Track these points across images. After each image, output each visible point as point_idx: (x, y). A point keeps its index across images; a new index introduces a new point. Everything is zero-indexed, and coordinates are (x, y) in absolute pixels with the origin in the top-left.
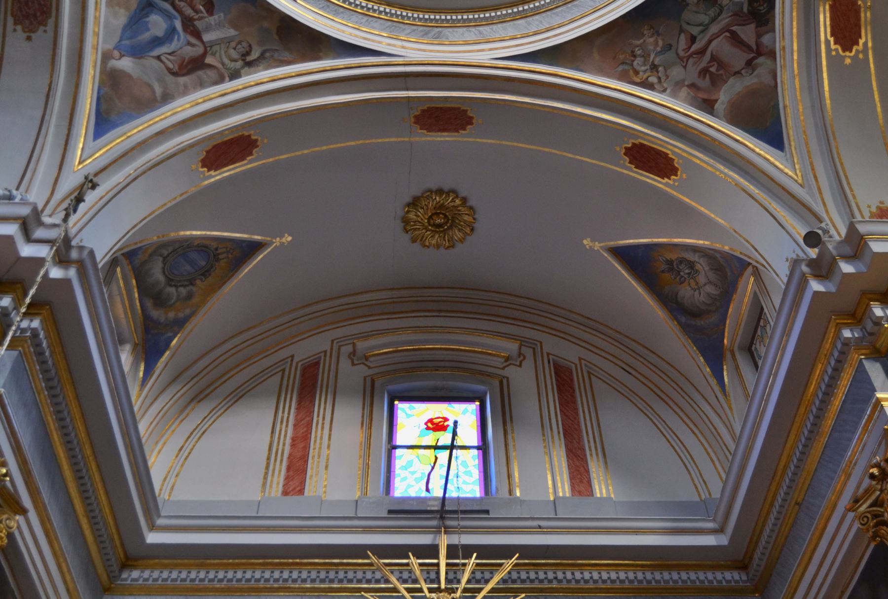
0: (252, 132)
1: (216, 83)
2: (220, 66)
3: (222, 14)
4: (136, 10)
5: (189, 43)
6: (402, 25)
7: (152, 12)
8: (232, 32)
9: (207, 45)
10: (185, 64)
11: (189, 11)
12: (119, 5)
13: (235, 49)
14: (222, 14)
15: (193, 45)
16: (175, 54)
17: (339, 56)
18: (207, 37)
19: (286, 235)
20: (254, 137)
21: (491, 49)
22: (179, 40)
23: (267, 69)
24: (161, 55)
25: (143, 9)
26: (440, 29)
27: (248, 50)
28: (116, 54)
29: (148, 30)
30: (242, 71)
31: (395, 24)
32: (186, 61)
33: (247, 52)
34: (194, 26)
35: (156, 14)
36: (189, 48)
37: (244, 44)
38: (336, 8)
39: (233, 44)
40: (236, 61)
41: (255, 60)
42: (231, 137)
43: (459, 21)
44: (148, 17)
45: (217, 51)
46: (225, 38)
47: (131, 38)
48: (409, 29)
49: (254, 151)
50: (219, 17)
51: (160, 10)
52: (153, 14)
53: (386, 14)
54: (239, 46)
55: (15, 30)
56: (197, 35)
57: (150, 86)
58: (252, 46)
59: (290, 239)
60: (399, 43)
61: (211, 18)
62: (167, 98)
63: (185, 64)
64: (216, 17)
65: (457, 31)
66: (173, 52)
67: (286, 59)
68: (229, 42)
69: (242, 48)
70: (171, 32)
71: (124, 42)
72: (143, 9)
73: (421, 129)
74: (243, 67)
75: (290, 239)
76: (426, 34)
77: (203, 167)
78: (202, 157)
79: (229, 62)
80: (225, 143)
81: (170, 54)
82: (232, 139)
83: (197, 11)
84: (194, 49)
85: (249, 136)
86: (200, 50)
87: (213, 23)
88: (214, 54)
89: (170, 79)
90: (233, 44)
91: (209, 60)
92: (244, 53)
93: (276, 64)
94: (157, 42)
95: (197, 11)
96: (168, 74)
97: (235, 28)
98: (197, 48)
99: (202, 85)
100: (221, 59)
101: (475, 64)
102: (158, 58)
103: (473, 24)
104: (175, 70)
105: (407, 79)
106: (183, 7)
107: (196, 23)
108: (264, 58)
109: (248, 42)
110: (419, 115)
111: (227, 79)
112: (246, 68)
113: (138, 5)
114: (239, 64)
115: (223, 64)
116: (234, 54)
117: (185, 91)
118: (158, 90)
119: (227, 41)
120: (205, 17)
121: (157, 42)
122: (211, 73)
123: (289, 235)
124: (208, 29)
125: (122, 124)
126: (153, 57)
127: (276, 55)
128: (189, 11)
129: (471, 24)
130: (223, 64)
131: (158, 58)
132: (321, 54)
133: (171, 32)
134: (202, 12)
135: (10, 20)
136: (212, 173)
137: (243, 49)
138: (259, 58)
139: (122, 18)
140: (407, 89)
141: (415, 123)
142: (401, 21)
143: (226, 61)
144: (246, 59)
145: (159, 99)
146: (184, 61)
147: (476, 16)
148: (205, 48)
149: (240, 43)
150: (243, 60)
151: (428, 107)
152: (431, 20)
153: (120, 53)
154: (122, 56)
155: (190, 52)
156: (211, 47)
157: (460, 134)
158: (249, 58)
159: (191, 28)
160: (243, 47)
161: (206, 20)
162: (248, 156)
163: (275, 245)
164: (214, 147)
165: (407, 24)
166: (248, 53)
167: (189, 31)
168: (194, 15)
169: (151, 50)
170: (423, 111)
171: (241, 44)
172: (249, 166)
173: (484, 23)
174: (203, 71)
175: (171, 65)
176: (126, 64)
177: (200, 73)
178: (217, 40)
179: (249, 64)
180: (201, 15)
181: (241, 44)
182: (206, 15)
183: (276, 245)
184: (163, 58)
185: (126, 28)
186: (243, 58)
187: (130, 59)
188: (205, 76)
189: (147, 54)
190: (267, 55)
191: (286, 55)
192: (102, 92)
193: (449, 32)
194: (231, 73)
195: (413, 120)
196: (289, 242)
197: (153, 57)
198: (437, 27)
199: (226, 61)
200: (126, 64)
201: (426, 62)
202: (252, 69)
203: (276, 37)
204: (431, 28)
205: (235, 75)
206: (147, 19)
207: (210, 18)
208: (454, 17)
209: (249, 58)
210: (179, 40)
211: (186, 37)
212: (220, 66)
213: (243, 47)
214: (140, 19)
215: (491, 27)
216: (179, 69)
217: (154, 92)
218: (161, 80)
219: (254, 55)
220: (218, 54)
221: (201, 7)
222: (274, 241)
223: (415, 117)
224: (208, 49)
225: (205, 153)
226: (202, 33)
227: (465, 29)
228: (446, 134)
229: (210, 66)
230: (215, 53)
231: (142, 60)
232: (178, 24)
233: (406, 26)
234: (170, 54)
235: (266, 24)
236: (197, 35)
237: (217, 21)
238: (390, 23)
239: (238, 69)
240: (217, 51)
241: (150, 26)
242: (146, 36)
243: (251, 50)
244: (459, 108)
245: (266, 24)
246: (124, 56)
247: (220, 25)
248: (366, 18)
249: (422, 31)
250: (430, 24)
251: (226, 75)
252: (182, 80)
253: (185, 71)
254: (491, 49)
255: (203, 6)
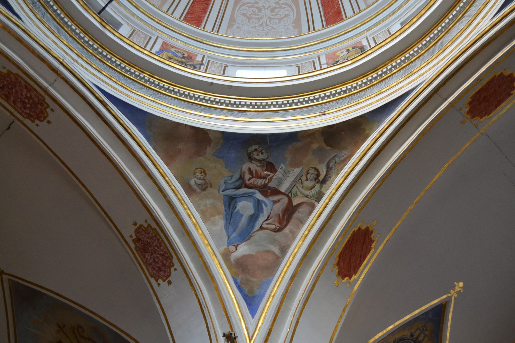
0: (359, 225)
1: (310, 213)
2: (305, 199)
3: (282, 165)
4: (225, 210)
5: (275, 202)
6: (412, 64)
7: (236, 202)
8: (298, 170)
9: (287, 194)
10: (281, 218)
11: (260, 182)
12: (212, 215)
13: (307, 180)
14: (282, 165)
15: (278, 201)
16: (271, 216)
17: (380, 122)
18: (283, 189)
19: (455, 283)
20: (364, 228)
21: (483, 18)
22: (266, 206)
23: (338, 174)
24: (262, 225)
25: (230, 205)
26: (441, 41)
27: (316, 173)
28: (232, 248)
29: (242, 215)
30: (323, 190)
31: (406, 68)
32: (281, 215)
33: (316, 175)
34: (269, 188)
35: (240, 201)
36: (277, 205)
37: (312, 171)
38: (358, 95)
39: (304, 178)
40: (313, 187)
41: (326, 176)
42: (347, 240)
43: (448, 23)
44: (236, 207)
45: (296, 192)
46: (296, 178)
47: (235, 230)
48: (418, 62)
49: (372, 237)
50: (282, 168)
51: (241, 197)
52: (238, 203)
53: (395, 67)
54: (309, 176)
55: (159, 285)
56: (276, 192)
57: (268, 251)
58: (317, 168)
59: (461, 284)
60: (416, 76)
61: (278, 173)
62: (284, 250)
63: (281, 218)
64: (279, 170)
65: (453, 32)
66: (268, 217)
67: (345, 156)
68: (300, 179)
69: (311, 176)
70: (258, 204)
71: (231, 237)
72: (230, 205)
73: (481, 118)
74: (321, 187)
75: (461, 284)
76: (433, 53)
77: (343, 278)
78: (337, 271)
79: (310, 191)
80: (346, 247)
81: (267, 220)
82: (349, 241)
83: (265, 178)
84: (280, 203)
85: (359, 229)
86: (285, 200)
87: (280, 176)
88: (296, 195)
89: (278, 236)
90: (304, 178)
91: (295, 203)
92: (315, 177)
93: (342, 166)
94: (253, 218)
95: (265, 178)
96: (276, 233)
97: (297, 165)
98: (282, 201)
99: (302, 222)
100: (303, 194)
101: (478, 37)
102: (261, 228)
103: (460, 16)
104: (278, 228)
105: (438, 92)
106: (254, 183)
107: (270, 185)
108: (331, 169)
109: (312, 167)
110: (470, 110)
111: (316, 203)
112: (324, 185)
113: (225, 206)
114: (318, 186)
115: (307, 196)
116: (309, 184)
117: (294, 235)
118: (276, 250)
119: (299, 179)
120: (273, 176)
121: (253, 218)
122: (303, 209)
123: (458, 282)
124: (280, 182)
125: (265, 291)
126: (258, 230)
127: (337, 159)
128: (260, 182)
129: (459, 17)
130: (307, 196)
131: (261, 228)
132: (367, 132)
133: (258, 204)
134: (269, 175)
135: (153, 280)
136: (354, 277)
137: (313, 175)
138: (327, 172)
139: (220, 222)
140: (446, 100)
141: (473, 117)
142: (409, 62)
143: (307, 192)
144: (319, 180)
145: (280, 255)
146: (279, 215)
147: (458, 9)
148: (287, 196)
149: (307, 173)
150: (317, 183)
151: (471, 98)
152: (429, 42)
153: (234, 245)
154: (236, 247)
155: (279, 208)
156: (291, 192)
157: (514, 95)
158: (321, 178)
159: (269, 191)
160: (312, 174)
161: (275, 177)
162: (371, 245)
163: (453, 298)
164: (340, 256)
165: (415, 60)
166: (318, 175)
167: (269, 194)
168: (265, 181)
169: (253, 227)
170: (470, 103)
171: (309, 173)
172: (378, 251)
173: (467, 8)
174: (297, 212)
175: (273, 227)
176: (243, 249)
177: (296, 215)
178: (291, 184)
179: (324, 181)
180: (268, 178)
181: (309, 173)
182: (272, 174)
183: (455, 297)
184: (264, 226)
185: (226, 227)
186: (317, 181)
187: (243, 244)
188: (301, 215)
189: (252, 232)
190: (331, 164)
191: (344, 153)
192: (239, 281)
193: (447, 37)
194: (316, 198)
195: (469, 117)
196: (463, 287)
197: (258, 230)
198: (437, 42)
199: (307, 192)
200: (243, 249)
201: (443, 69)
202: (328, 183)
203: (329, 148)
204: (433, 47)
205: (319, 196)
206: (237, 209)
207: (276, 174)
208: (443, 25)
209: (321, 178)
210: (266, 206)
211: (269, 200)
212: (305, 199)
213: (312, 174)
214: (232, 213)
215: (474, 5)
216: (280, 223)
217: (274, 253)
218: (274, 242)
219: (323, 172)
220: (298, 193)
221: (265, 172)
222: (449, 295)
223: (469, 112)
224: (290, 195)
225: (337, 267)
226: (278, 188)
227: (457, 25)
228: (503, 104)
229: (299, 205)
230: (296, 193)
231: (252, 239)
232: (259, 196)
233: (416, 62)
234: (267, 220)
235: (315, 146)
236: (276, 192)
237: (283, 172)
238: (402, 71)
239: (319, 191)
240: (296, 192)
241: (241, 212)
242: (244, 221)
243: (318, 172)
244: (495, 77)
245: (315, 146)
246: (237, 245)
247: (286, 173)
248: (383, 83)
249: (428, 55)
250: (431, 45)
251: (314, 201)
252: (287, 230)
253: (285, 223)
254: (483, 18)
255: (265, 171)
